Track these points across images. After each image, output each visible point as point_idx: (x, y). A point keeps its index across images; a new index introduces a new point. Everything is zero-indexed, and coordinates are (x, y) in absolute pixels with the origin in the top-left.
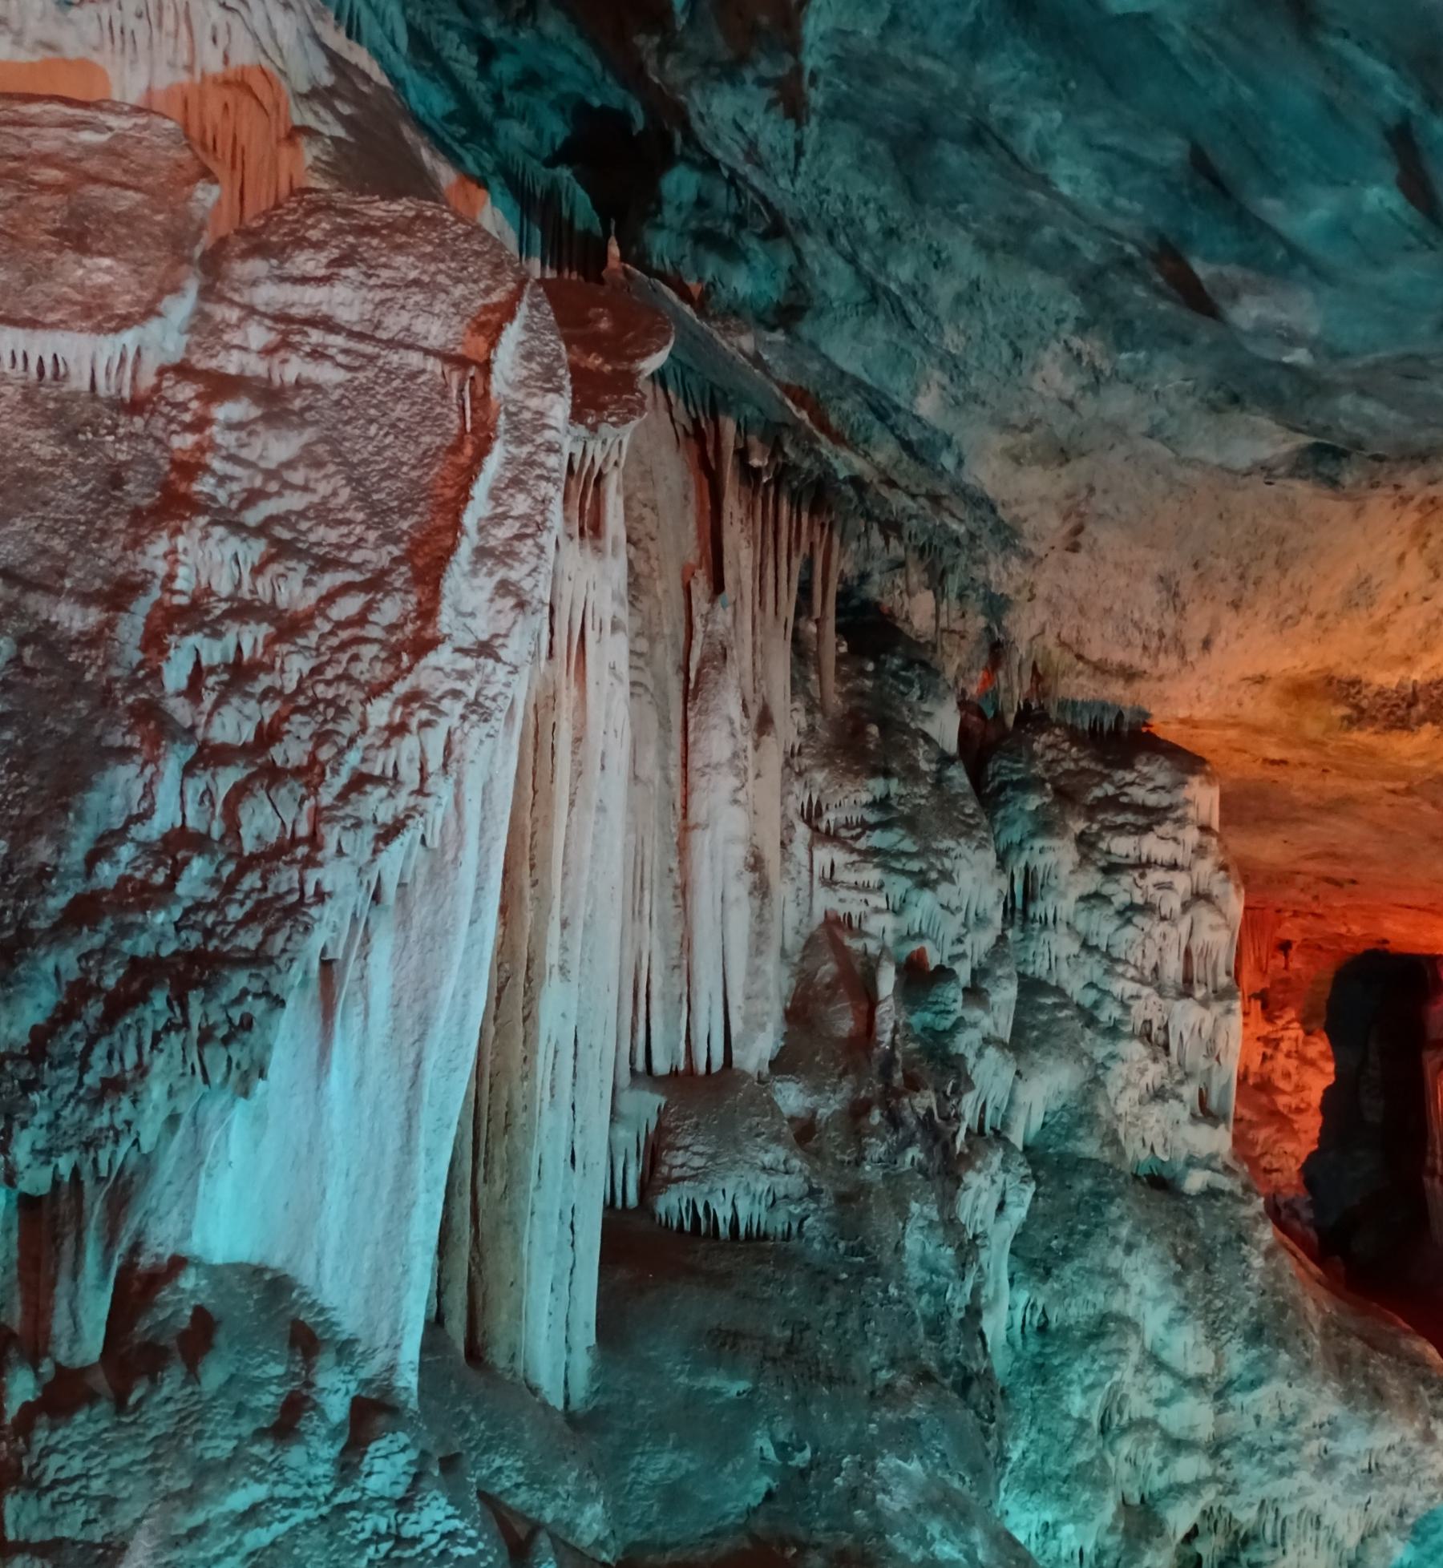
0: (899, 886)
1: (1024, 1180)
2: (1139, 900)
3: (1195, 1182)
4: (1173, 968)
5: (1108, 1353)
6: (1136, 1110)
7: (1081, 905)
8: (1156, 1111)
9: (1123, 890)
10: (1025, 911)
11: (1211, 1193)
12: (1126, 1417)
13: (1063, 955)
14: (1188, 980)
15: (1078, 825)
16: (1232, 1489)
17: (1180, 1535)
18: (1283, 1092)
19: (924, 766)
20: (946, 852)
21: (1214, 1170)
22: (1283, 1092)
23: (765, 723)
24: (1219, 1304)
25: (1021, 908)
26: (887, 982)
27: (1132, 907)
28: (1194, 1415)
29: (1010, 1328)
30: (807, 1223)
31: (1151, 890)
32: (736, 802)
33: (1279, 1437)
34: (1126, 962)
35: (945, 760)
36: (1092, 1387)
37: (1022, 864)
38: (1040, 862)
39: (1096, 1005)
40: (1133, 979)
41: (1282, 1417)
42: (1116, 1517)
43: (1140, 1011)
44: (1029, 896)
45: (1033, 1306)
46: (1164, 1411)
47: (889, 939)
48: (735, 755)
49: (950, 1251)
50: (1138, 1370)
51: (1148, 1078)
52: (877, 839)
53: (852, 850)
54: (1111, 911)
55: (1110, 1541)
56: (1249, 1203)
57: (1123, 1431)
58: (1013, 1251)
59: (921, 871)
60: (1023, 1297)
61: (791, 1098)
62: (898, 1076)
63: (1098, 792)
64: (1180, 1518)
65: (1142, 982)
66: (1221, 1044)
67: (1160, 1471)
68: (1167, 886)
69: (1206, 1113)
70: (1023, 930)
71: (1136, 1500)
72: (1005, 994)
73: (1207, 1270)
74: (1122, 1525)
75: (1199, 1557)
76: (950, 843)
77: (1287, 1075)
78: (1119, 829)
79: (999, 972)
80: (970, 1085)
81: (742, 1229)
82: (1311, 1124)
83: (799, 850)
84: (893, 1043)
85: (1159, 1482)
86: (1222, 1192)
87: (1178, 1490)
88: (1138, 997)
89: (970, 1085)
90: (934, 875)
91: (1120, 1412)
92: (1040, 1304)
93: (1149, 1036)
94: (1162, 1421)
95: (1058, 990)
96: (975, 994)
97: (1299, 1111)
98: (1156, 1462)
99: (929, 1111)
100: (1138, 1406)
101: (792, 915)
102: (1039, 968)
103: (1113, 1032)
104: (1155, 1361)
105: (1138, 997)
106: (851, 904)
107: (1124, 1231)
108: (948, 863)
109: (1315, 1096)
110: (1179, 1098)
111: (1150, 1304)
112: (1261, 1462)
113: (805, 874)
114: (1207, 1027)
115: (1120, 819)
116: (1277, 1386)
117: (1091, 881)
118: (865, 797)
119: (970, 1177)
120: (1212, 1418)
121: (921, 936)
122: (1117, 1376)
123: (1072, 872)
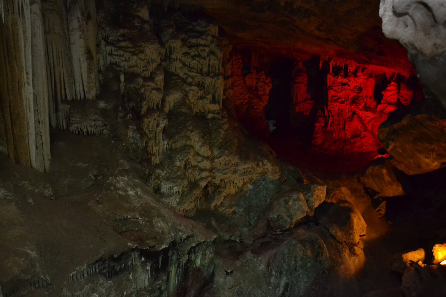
0: (127, 55)
1: (164, 119)
2: (197, 54)
3: (210, 116)
4: (205, 69)
5: (185, 153)
6: (196, 101)
7: (183, 55)
8: (201, 101)
9: (193, 52)
10: (170, 57)
11: (214, 118)
12: (190, 165)
13: (178, 67)
14: (209, 72)
15: (183, 36)
16: (214, 178)
17: (203, 187)
18: (260, 91)
19: (137, 24)
20: (142, 46)
21: (215, 114)
22: (260, 91)
23: (88, 18)
24: (213, 141)
25: (167, 57)
26: (122, 78)
27: (196, 56)
28: (206, 164)
29: (163, 149)
30: (104, 131)
31: (200, 51)
32: (81, 38)
33: (225, 167)
34: (194, 68)
35: (144, 22)
36: (182, 160)
37: (168, 46)
38: (172, 45)
39: (187, 78)
40: (195, 72)
41: (226, 163)
42: (188, 185)
43: (197, 80)
44: (171, 53)
45: (169, 144)
46: (199, 164)
47: (126, 67)
48: (80, 26)
49: (139, 135)
50: (193, 156)
51: (199, 94)
52: (123, 44)
53: (116, 47)
54: (190, 56)
55: (185, 189)
56: (222, 120)
57: (190, 168)
58: (163, 133)
59: (134, 51)
60: (166, 143)
61: (102, 105)
62: (126, 99)
63: (188, 28)
64: (203, 184)
65: (198, 73)
66: (216, 86)
67: (199, 175)
68: (204, 50)
69: (214, 101)
70: (169, 61)
71: (194, 181)
72: (160, 78)
73: (210, 135)
74: (189, 186)
75: (208, 191)
76: (143, 44)
77: (261, 87)
78: (193, 37)
79: (158, 73)
80: (145, 100)
81: (90, 133)
82: (266, 98)
83: (103, 47)
84: (124, 92)
85: (198, 177)
86: (216, 118)
87: (202, 179)
88: (196, 76)
89: (145, 100)
90: (137, 52)
91: (189, 164)
92: (170, 143)
93: (200, 86)
94: (199, 165)
95: (178, 75)
96: (151, 78)
97: (264, 95)
98: (198, 174)
99: (133, 106)
100: (194, 163)
101: (102, 62)
102: (173, 70)
103: (190, 84)
104: (198, 154)
105: (196, 76)
106: (117, 59)
107: (191, 128)
108: (142, 48)
109: (268, 92)
110: (206, 98)
111: (196, 143)
112: (221, 172)
113: (105, 52)
114: (213, 82)
115: (193, 34)
116: (224, 157)
117: (185, 49)
118: (119, 34)
119: (145, 120)
120: (210, 164)
121: (134, 66)
122: (187, 157)
123: (180, 48)
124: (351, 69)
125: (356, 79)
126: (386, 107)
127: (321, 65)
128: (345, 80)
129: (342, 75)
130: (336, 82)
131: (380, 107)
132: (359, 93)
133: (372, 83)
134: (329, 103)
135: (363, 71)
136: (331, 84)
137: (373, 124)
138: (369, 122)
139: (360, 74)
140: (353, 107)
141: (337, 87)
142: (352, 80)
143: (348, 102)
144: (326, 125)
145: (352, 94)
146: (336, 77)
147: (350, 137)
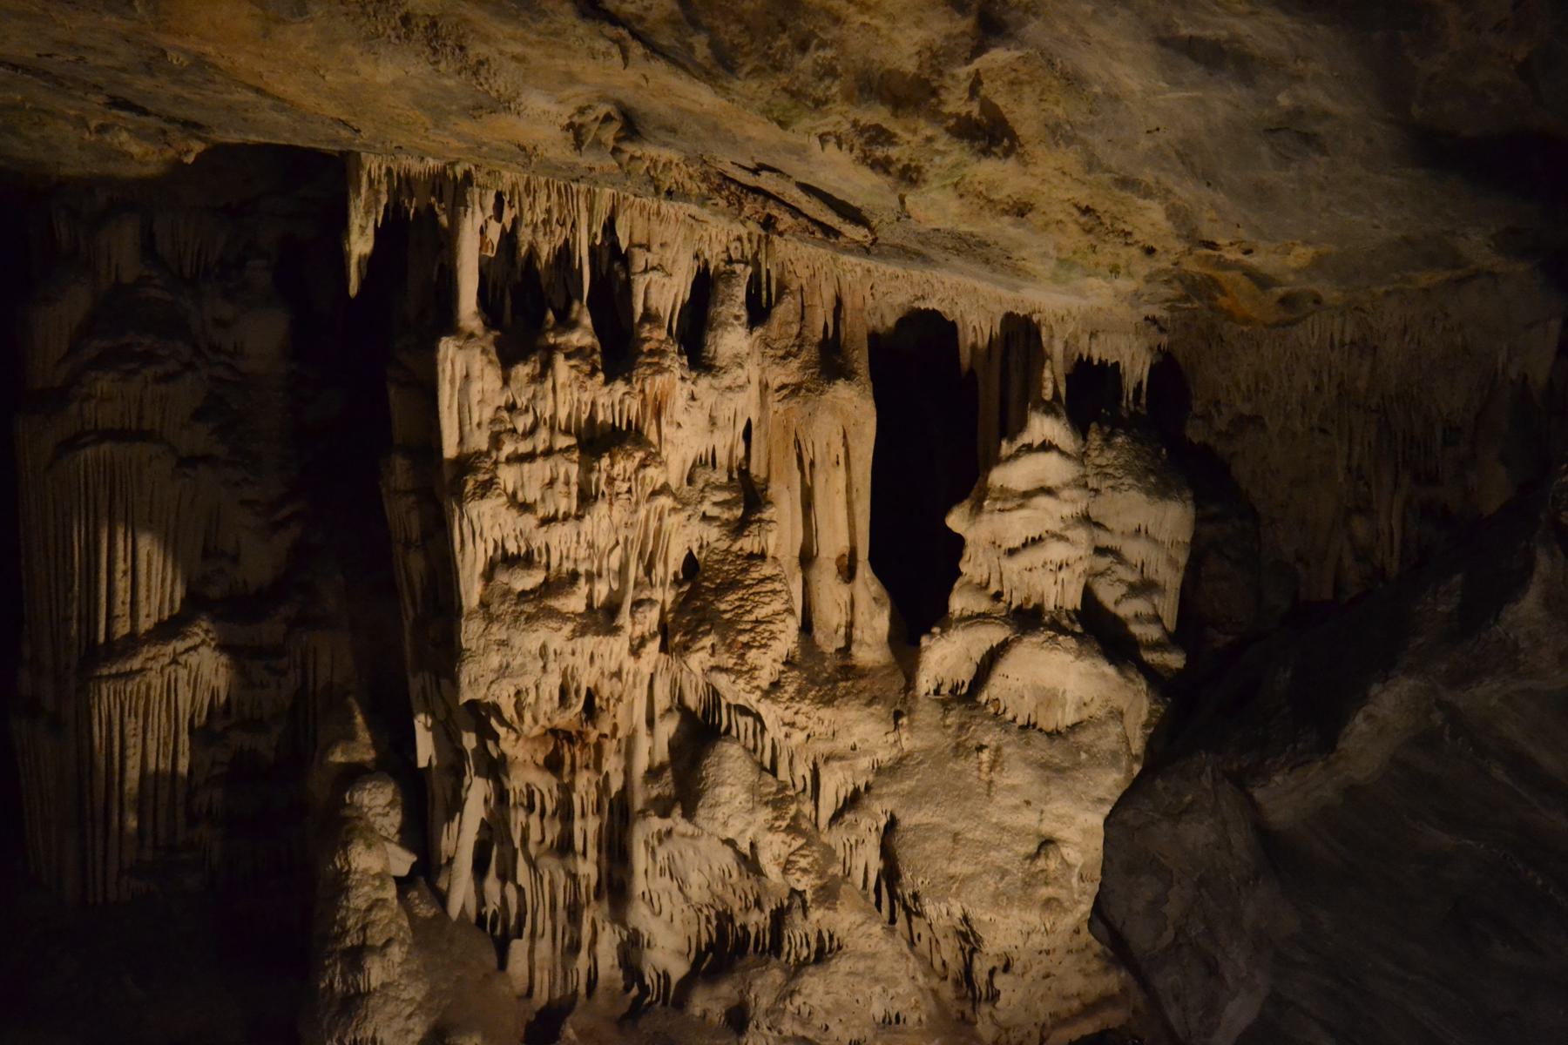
124: (663, 291)
125: (704, 382)
126: (993, 657)
127: (360, 244)
128: (613, 401)
129: (579, 353)
130: (524, 422)
131: (946, 657)
132: (738, 529)
133: (849, 417)
134: (471, 632)
135: (758, 313)
136: (480, 441)
137: (892, 824)
138: (853, 801)
139: (732, 340)
140: (698, 660)
141: (540, 470)
142: (680, 393)
143: (651, 617)
144: (429, 868)
145: (685, 536)
146: (523, 371)
147: (678, 969)
